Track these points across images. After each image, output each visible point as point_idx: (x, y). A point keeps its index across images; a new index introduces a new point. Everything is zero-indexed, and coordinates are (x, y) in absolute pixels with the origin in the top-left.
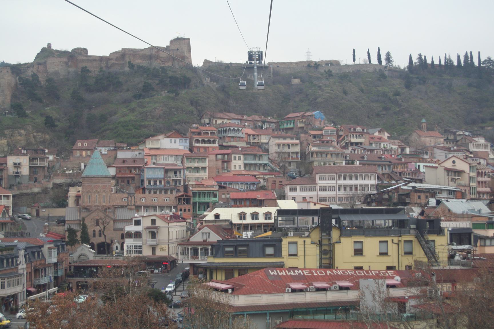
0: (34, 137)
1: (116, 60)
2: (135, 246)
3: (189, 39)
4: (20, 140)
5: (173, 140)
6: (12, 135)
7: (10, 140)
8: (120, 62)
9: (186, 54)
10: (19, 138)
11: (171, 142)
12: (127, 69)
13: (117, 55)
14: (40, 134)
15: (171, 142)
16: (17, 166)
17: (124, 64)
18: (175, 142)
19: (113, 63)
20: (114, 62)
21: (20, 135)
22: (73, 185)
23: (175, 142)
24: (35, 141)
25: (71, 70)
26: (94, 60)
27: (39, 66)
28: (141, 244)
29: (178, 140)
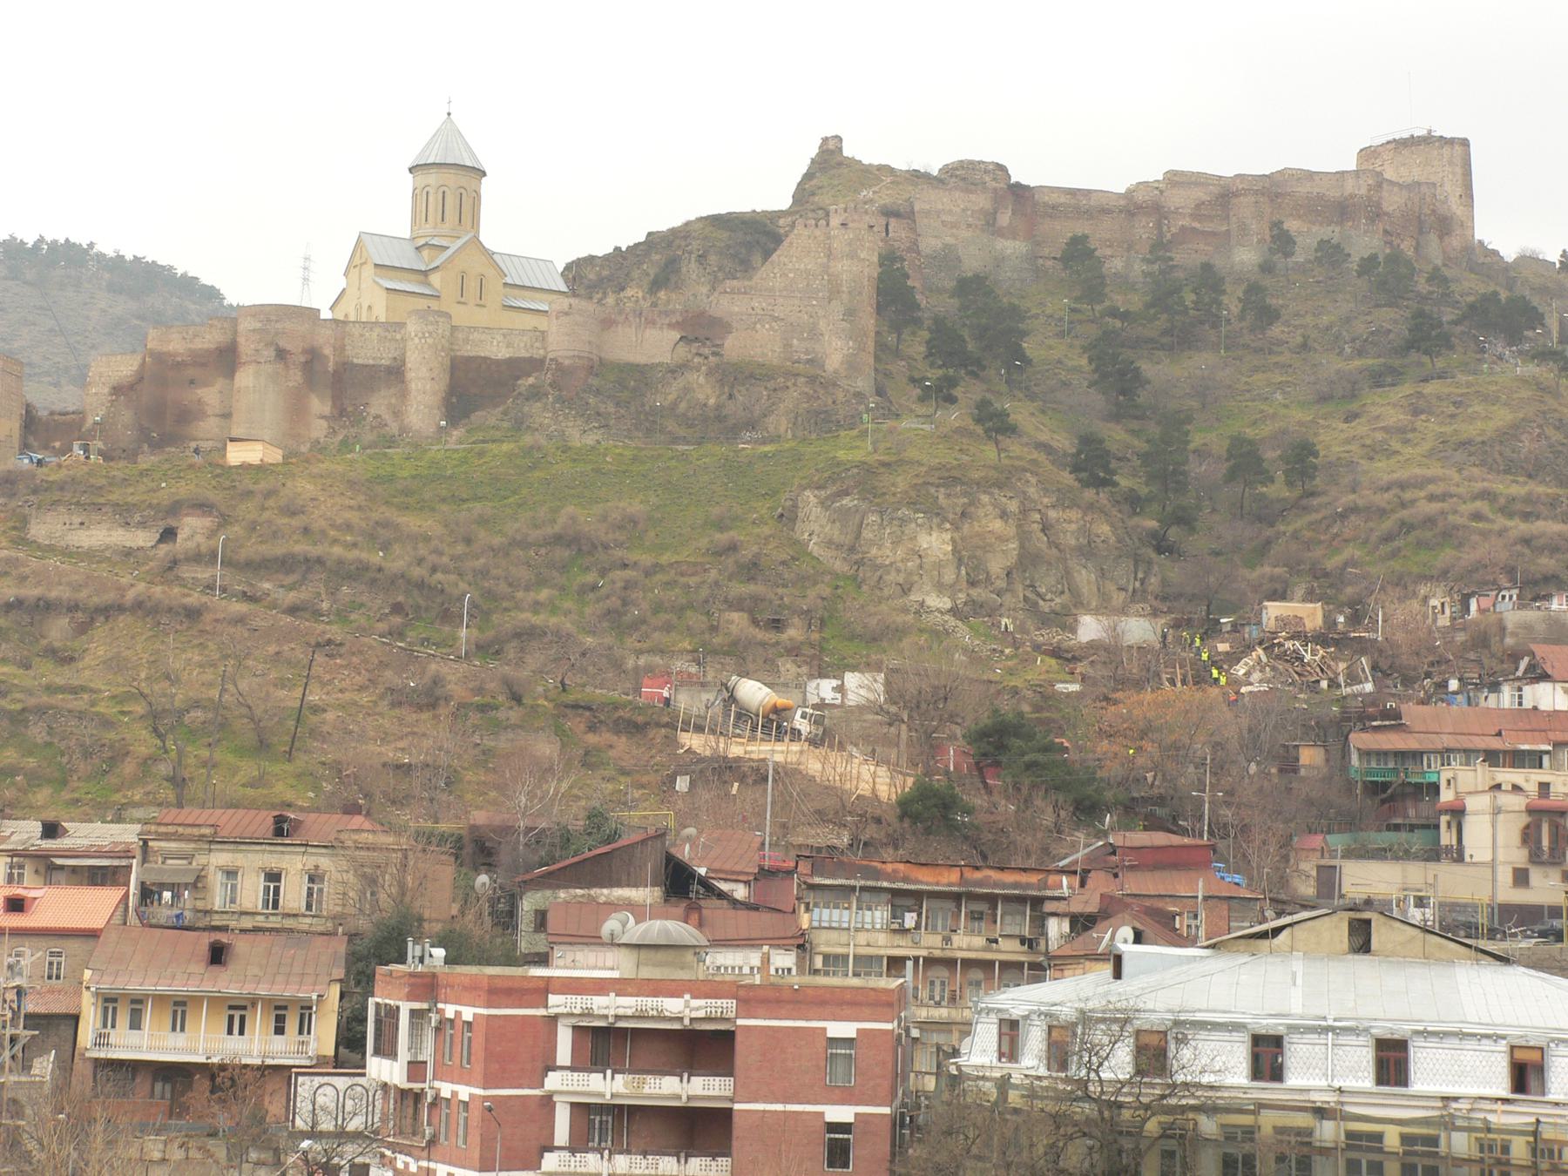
0: (1046, 528)
1: (1194, 216)
3: (1465, 143)
4: (1002, 539)
6: (963, 514)
7: (956, 535)
8: (1209, 227)
9: (1456, 208)
10: (997, 525)
14: (1074, 514)
20: (1186, 222)
21: (1004, 515)
24: (1053, 544)
25: (1013, 248)
26: (1105, 211)
27: (893, 222)
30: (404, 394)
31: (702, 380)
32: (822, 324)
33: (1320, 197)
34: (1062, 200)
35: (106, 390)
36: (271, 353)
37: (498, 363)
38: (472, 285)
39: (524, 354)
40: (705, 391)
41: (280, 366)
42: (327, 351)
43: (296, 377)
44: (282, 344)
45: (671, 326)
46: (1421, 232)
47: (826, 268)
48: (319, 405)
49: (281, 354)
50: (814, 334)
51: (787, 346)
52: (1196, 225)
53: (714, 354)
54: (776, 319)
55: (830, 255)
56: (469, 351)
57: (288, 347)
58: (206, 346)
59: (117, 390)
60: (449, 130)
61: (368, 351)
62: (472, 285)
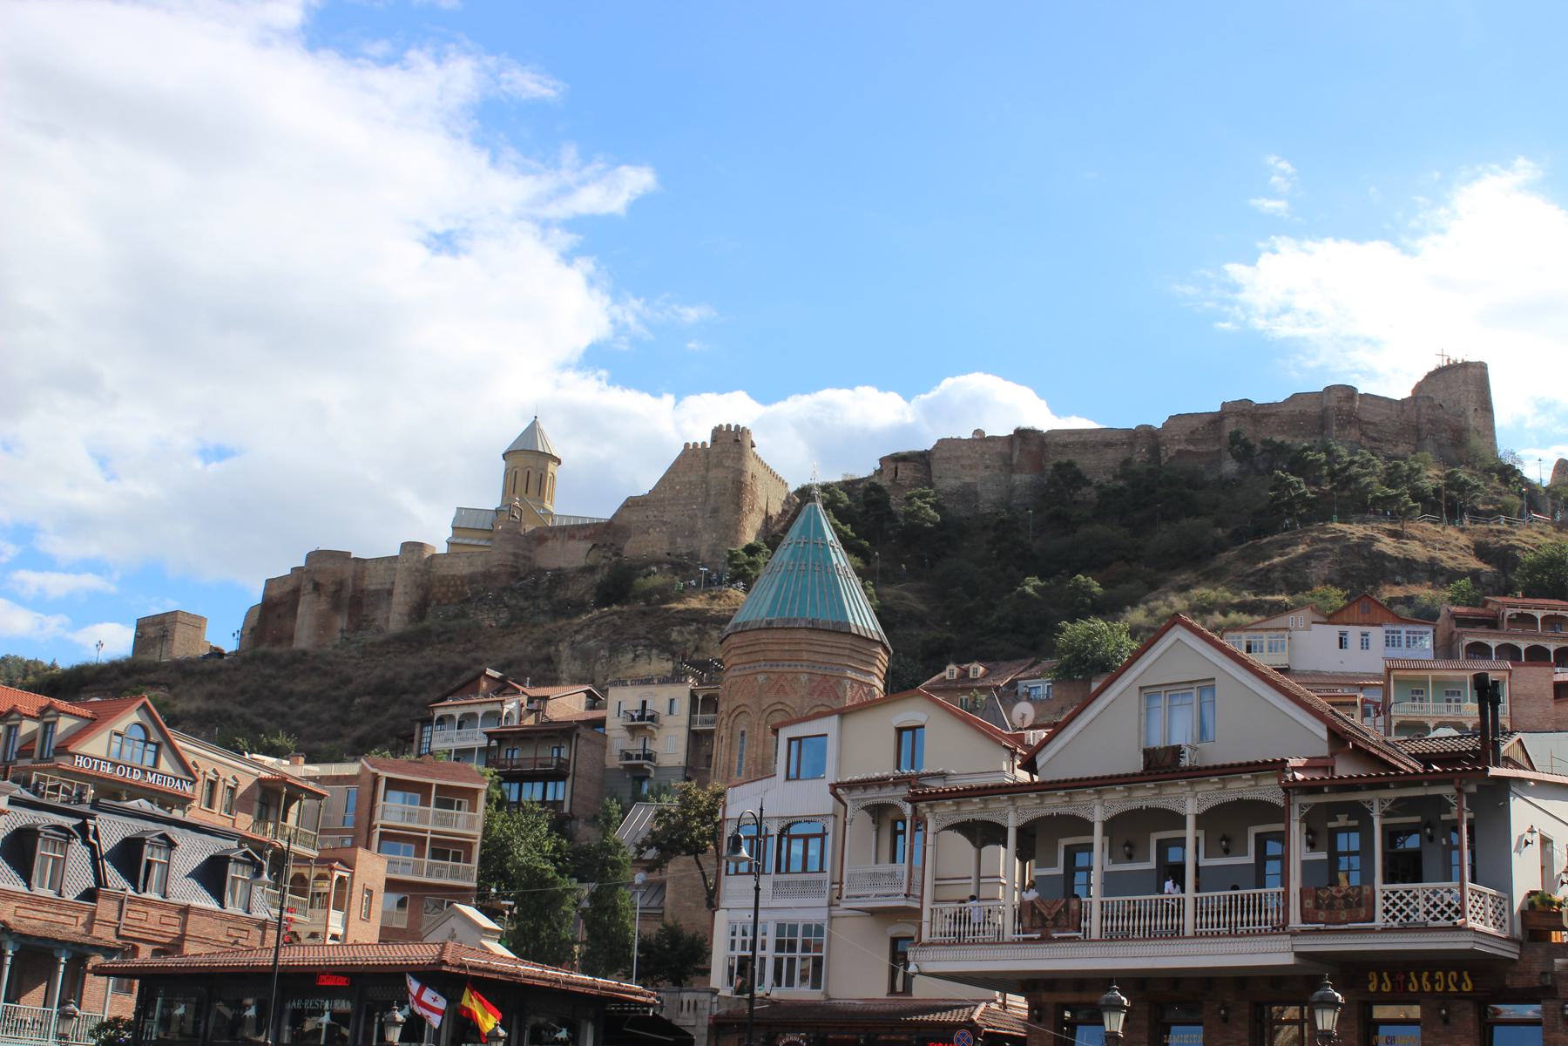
1: (1188, 441)
2: (780, 928)
5: (1354, 633)
8: (1202, 448)
11: (1342, 644)
12: (1230, 467)
13: (1195, 423)
15: (1342, 644)
16: (643, 722)
17: (1219, 451)
18: (1365, 645)
19: (1179, 452)
20: (1182, 447)
22: (704, 703)
23: (1365, 645)
28: (819, 916)
29: (1377, 634)
37: (462, 578)
39: (481, 569)
46: (1419, 440)
51: (672, 543)
52: (1191, 448)
53: (616, 554)
60: (533, 430)
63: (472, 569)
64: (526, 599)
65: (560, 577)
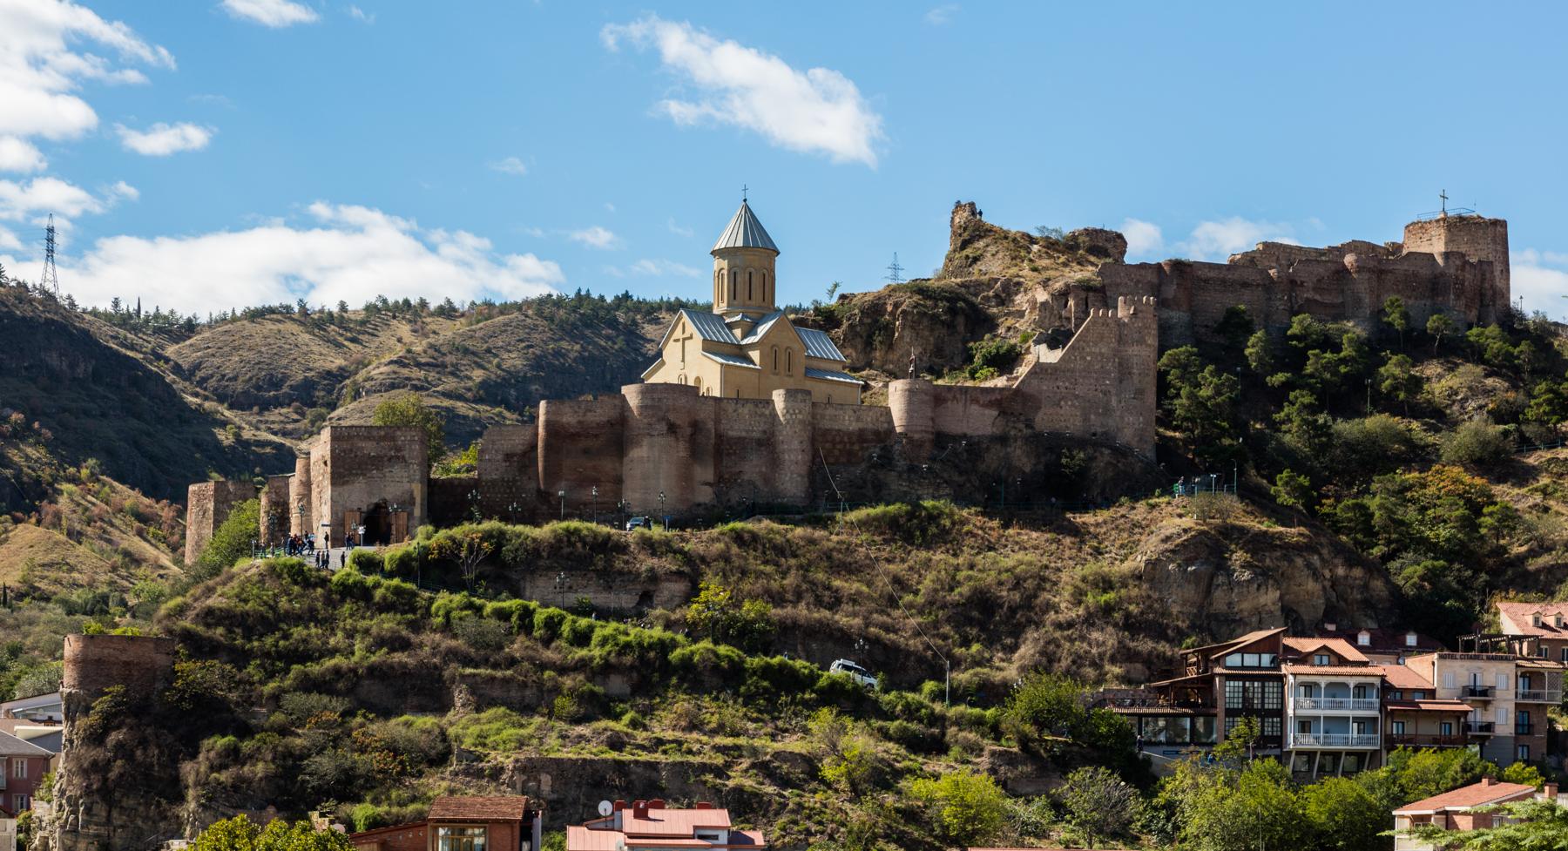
19: (1308, 300)
30: (775, 462)
31: (1018, 452)
32: (1114, 402)
33: (1415, 275)
34: (1212, 274)
35: (500, 457)
36: (663, 427)
38: (783, 358)
40: (1022, 459)
41: (671, 439)
42: (711, 425)
43: (681, 450)
44: (672, 417)
45: (990, 405)
47: (1116, 353)
48: (705, 473)
49: (672, 429)
50: (1107, 411)
51: (1086, 419)
52: (1318, 297)
54: (1077, 397)
55: (1120, 340)
56: (826, 424)
57: (679, 422)
58: (597, 419)
59: (508, 457)
61: (741, 425)
62: (783, 358)
63: (860, 425)
64: (961, 474)
65: (975, 448)
